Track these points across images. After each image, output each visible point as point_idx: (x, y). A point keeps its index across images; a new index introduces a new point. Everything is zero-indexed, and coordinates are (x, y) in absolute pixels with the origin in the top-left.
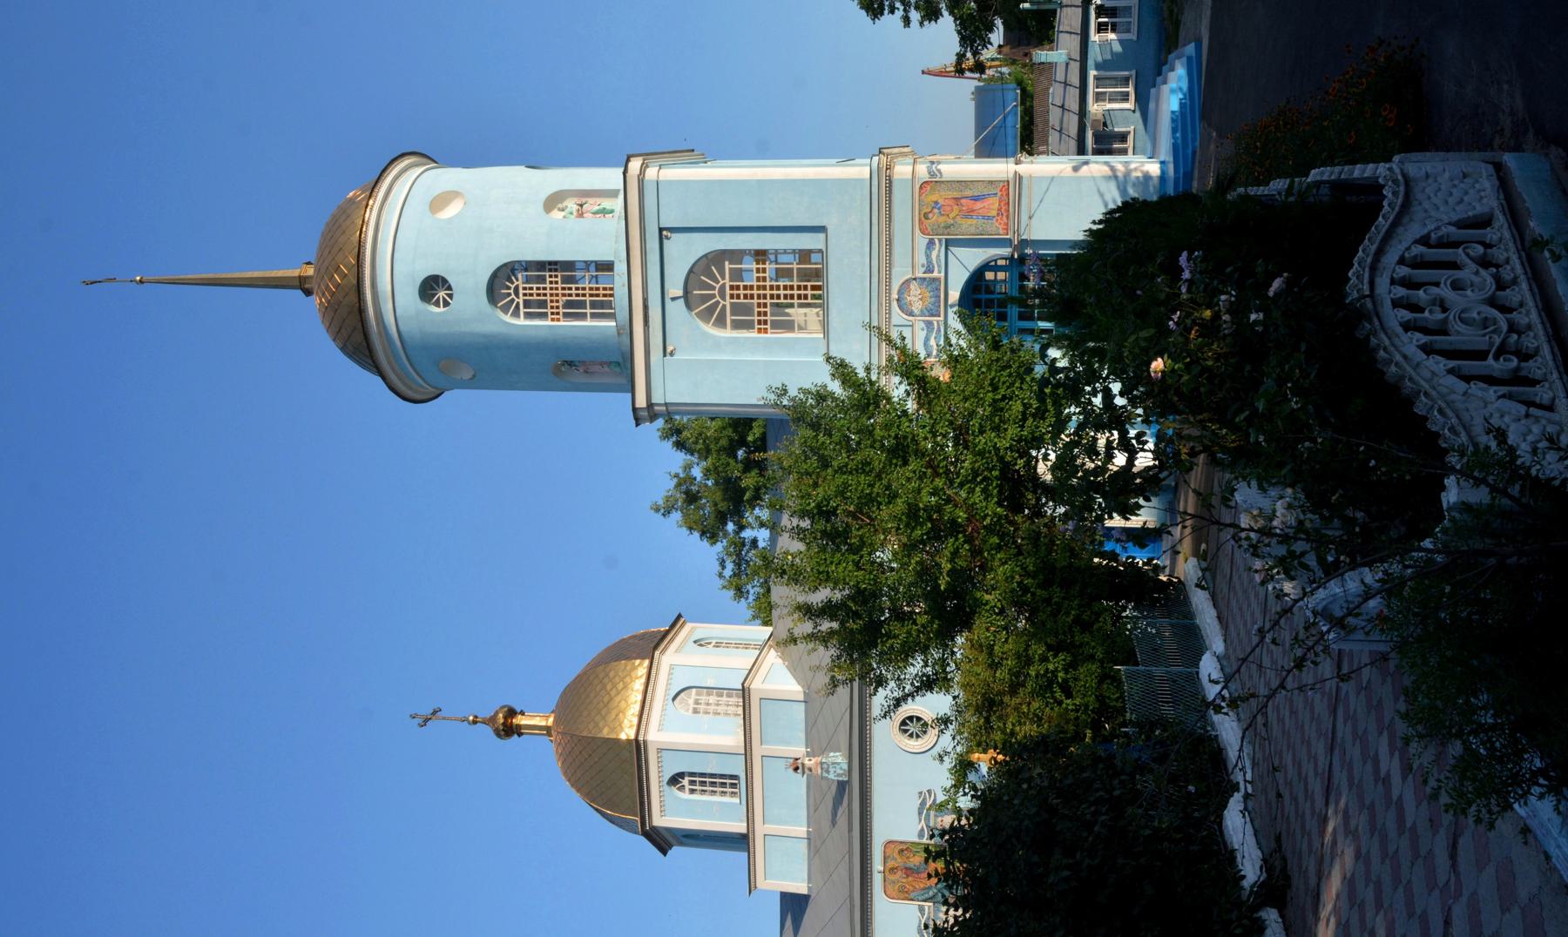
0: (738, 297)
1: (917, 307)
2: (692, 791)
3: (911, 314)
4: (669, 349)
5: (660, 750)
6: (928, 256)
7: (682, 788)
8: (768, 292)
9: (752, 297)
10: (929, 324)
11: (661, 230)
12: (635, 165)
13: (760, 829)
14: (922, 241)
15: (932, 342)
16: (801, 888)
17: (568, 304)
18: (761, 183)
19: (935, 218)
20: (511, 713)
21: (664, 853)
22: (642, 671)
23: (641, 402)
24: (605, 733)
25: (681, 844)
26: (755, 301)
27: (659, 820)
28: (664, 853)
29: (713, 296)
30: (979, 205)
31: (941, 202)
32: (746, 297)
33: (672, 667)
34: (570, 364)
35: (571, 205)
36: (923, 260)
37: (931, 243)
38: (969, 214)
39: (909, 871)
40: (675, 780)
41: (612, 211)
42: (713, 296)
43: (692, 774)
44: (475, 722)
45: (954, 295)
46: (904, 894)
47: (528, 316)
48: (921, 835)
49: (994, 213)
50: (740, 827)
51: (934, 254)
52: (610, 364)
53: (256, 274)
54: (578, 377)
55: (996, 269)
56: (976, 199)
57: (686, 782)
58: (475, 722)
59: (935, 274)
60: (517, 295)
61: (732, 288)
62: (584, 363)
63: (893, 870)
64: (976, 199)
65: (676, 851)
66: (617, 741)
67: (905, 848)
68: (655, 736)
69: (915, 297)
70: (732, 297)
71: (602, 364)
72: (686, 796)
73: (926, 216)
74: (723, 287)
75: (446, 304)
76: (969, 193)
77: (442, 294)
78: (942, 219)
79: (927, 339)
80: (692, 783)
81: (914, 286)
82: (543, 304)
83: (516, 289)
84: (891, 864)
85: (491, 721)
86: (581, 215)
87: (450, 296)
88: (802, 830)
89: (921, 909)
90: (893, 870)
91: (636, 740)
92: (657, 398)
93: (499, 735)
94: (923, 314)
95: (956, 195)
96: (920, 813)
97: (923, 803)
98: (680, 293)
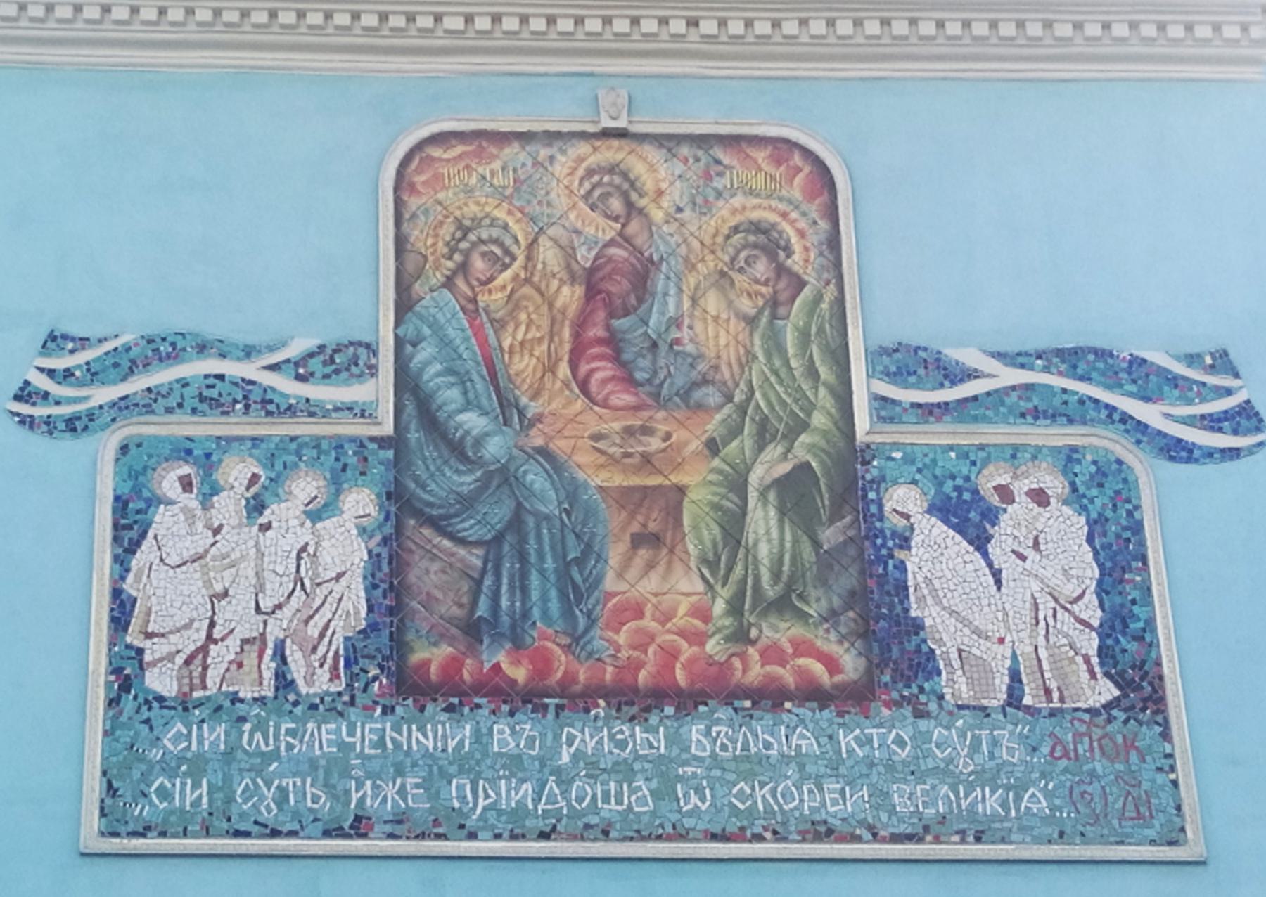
39: (615, 292)
48: (906, 362)
89: (343, 359)
90: (621, 196)
96: (1071, 359)
97: (1142, 376)
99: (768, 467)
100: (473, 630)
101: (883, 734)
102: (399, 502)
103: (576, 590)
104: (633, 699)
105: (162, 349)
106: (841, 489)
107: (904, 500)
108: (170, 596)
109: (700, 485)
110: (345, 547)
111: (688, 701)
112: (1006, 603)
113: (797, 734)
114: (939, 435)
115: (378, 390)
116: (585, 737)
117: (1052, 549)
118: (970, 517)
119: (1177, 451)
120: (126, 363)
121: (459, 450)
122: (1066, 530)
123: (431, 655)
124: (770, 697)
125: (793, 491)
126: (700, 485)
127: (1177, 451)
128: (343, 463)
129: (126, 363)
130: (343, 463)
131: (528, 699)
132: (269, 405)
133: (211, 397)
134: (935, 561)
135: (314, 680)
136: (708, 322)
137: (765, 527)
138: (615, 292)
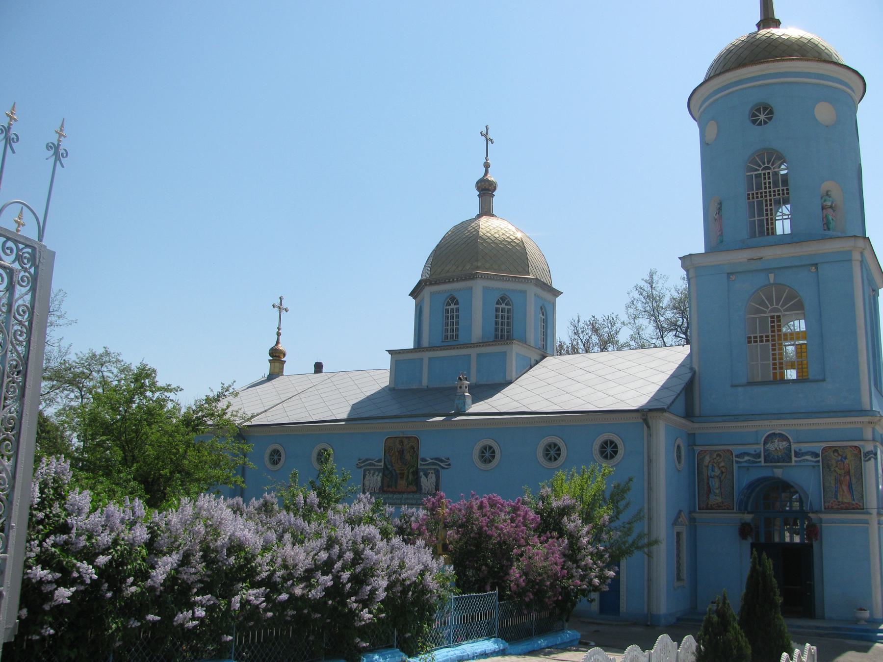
0: (773, 322)
1: (771, 447)
2: (447, 311)
3: (765, 443)
4: (733, 277)
5: (471, 288)
6: (806, 453)
8: (776, 342)
9: (773, 331)
10: (758, 455)
11: (816, 265)
14: (818, 447)
15: (747, 458)
17: (760, 204)
18: (854, 333)
21: (411, 295)
26: (770, 334)
28: (411, 295)
29: (772, 304)
30: (845, 488)
31: (846, 461)
32: (773, 327)
33: (525, 292)
34: (720, 209)
37: (817, 455)
38: (838, 482)
39: (401, 452)
40: (453, 300)
41: (829, 229)
42: (772, 304)
43: (458, 310)
44: (487, 166)
45: (779, 473)
46: (388, 450)
48: (424, 460)
49: (840, 499)
51: (808, 457)
52: (721, 235)
55: (801, 501)
57: (452, 306)
59: (794, 459)
60: (764, 169)
61: (779, 317)
62: (721, 217)
63: (402, 442)
65: (412, 302)
67: (414, 450)
68: (478, 286)
69: (777, 446)
70: (772, 317)
71: (721, 230)
73: (836, 451)
74: (779, 311)
76: (854, 481)
77: (762, 117)
78: (834, 462)
79: (748, 454)
80: (452, 310)
82: (759, 187)
83: (768, 168)
84: (405, 441)
87: (760, 124)
88: (425, 382)
90: (402, 442)
93: (477, 183)
94: (765, 450)
95: (852, 471)
96: (436, 459)
97: (442, 461)
98: (772, 281)
99: (411, 470)
100: (388, 486)
101: (417, 496)
102: (384, 475)
103: (396, 483)
104: (400, 493)
105: (367, 460)
106: (416, 473)
107: (422, 473)
108: (367, 483)
109: (406, 472)
110: (379, 479)
111: (404, 493)
112: (427, 483)
113: (411, 496)
114: (426, 467)
115: (382, 464)
116: (396, 496)
117: (432, 477)
118: (426, 475)
119: (443, 468)
120: (364, 462)
121: (388, 469)
122: (434, 476)
123: (385, 489)
124: (409, 493)
125: (413, 473)
126: (406, 472)
127: (443, 468)
128: (379, 470)
129: (364, 462)
130: (379, 470)
131: (392, 492)
132: (375, 465)
133: (371, 464)
134: (423, 479)
135: (377, 491)
136: (408, 456)
137: (410, 477)
138: (401, 452)
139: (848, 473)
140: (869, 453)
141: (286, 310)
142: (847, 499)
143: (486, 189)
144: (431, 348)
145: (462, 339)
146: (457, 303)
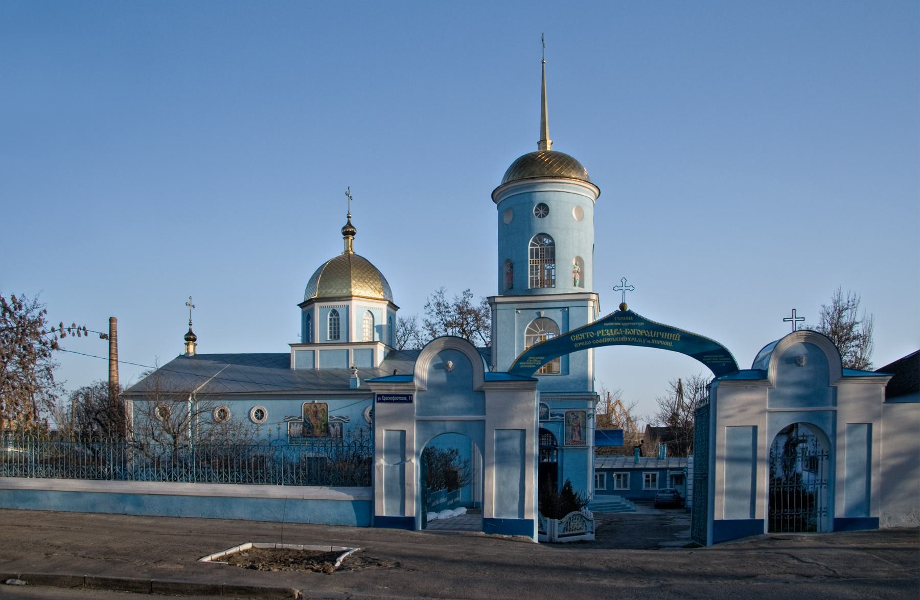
5: (348, 307)
7: (331, 315)
12: (594, 297)
13: (317, 349)
14: (563, 412)
16: (294, 365)
19: (572, 416)
20: (353, 234)
21: (299, 305)
22: (381, 297)
23: (497, 300)
24: (353, 282)
25: (303, 313)
27: (317, 306)
34: (512, 267)
35: (577, 268)
36: (556, 411)
37: (562, 416)
38: (573, 430)
39: (316, 413)
40: (334, 312)
44: (348, 217)
46: (306, 411)
47: (532, 250)
50: (317, 341)
53: (547, 127)
54: (506, 269)
56: (579, 432)
58: (348, 217)
64: (579, 432)
66: (350, 287)
67: (325, 411)
72: (329, 317)
75: (536, 214)
81: (546, 409)
85: (349, 223)
86: (574, 272)
91: (352, 296)
92: (499, 306)
93: (344, 228)
136: (320, 415)
138: (316, 413)
139: (579, 425)
140: (589, 415)
141: (194, 307)
142: (578, 439)
143: (348, 232)
144: (320, 344)
145: (343, 339)
146: (338, 315)
